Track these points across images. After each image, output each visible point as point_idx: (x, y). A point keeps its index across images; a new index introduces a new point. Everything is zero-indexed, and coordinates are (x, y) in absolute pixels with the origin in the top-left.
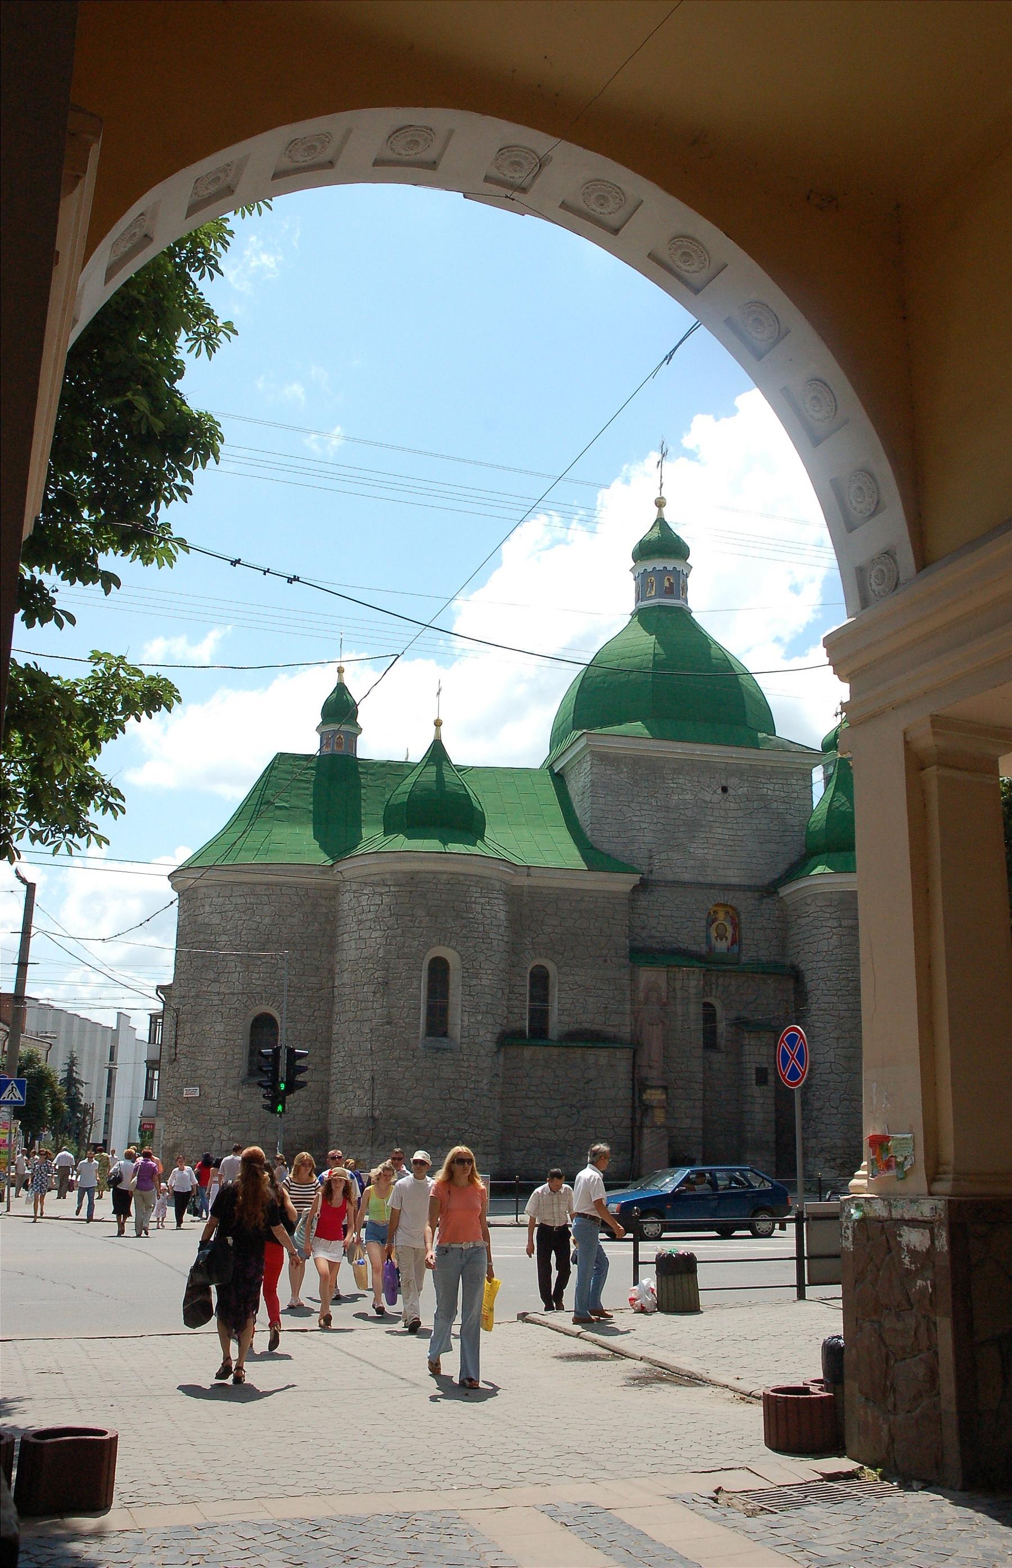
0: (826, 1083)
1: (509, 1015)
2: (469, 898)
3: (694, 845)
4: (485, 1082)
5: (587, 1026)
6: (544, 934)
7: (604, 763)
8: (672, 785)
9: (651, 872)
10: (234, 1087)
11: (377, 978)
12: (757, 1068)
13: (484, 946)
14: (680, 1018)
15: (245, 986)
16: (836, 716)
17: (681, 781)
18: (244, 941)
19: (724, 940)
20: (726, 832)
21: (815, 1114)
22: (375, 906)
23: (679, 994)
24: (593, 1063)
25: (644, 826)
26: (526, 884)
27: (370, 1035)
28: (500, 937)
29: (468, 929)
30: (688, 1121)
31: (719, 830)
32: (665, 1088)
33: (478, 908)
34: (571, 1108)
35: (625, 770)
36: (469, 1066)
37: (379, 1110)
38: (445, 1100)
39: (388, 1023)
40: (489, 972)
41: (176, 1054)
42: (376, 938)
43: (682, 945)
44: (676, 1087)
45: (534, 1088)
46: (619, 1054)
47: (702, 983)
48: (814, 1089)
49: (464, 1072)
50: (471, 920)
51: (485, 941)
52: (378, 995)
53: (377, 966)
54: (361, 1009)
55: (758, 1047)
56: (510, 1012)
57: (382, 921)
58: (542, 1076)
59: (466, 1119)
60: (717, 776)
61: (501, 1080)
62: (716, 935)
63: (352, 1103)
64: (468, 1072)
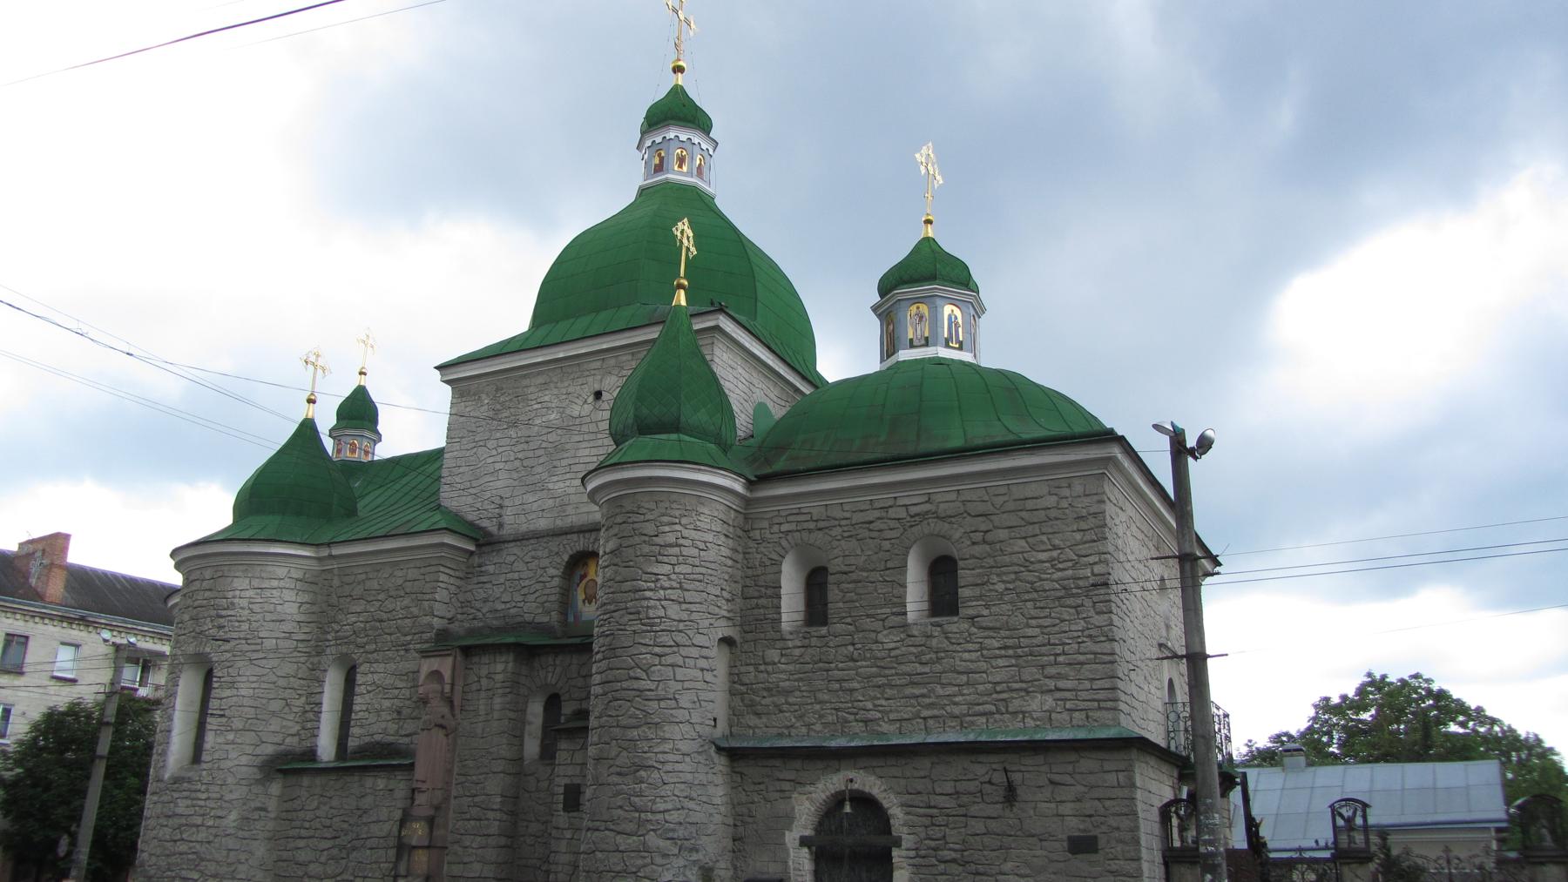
1: (302, 732)
2: (231, 593)
3: (555, 479)
4: (233, 816)
5: (378, 738)
6: (348, 625)
7: (464, 399)
8: (536, 406)
9: (501, 526)
12: (566, 786)
13: (246, 647)
14: (481, 719)
17: (547, 398)
19: (593, 603)
20: (594, 451)
23: (484, 682)
24: (370, 788)
25: (498, 466)
26: (335, 566)
28: (284, 635)
29: (227, 629)
30: (477, 867)
31: (587, 452)
32: (431, 821)
33: (244, 603)
34: (340, 850)
35: (486, 401)
36: (208, 799)
38: (175, 841)
40: (255, 679)
43: (528, 618)
44: (468, 817)
45: (307, 825)
46: (400, 775)
47: (511, 665)
49: (202, 807)
50: (230, 618)
51: (249, 642)
55: (571, 752)
56: (303, 728)
58: (318, 808)
59: (197, 866)
60: (590, 379)
61: (272, 815)
62: (584, 597)
64: (206, 806)
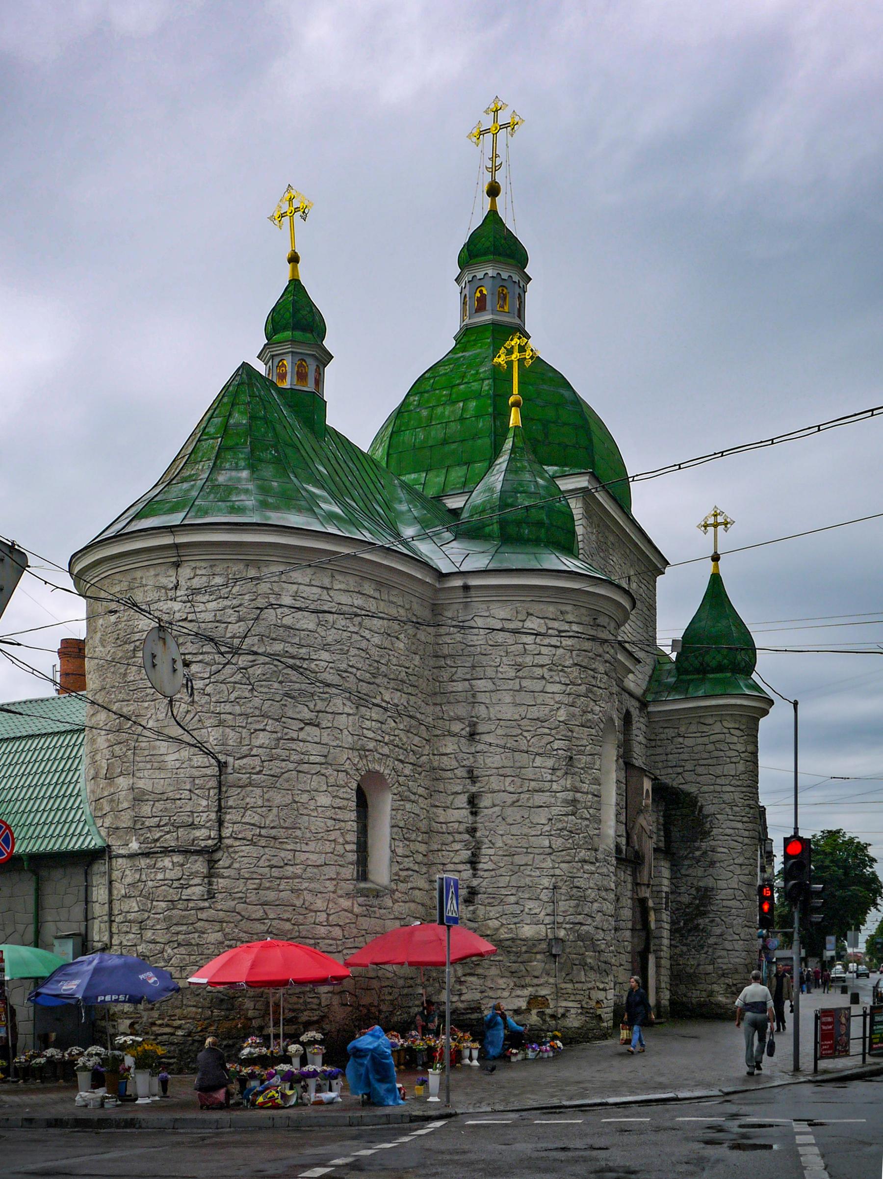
0: (729, 910)
10: (348, 895)
11: (556, 750)
15: (356, 738)
16: (706, 526)
18: (352, 666)
21: (712, 940)
22: (550, 648)
27: (547, 828)
37: (565, 928)
39: (573, 814)
41: (221, 838)
42: (553, 693)
48: (711, 916)
52: (559, 773)
53: (557, 733)
54: (528, 791)
57: (562, 671)
63: (516, 920)
